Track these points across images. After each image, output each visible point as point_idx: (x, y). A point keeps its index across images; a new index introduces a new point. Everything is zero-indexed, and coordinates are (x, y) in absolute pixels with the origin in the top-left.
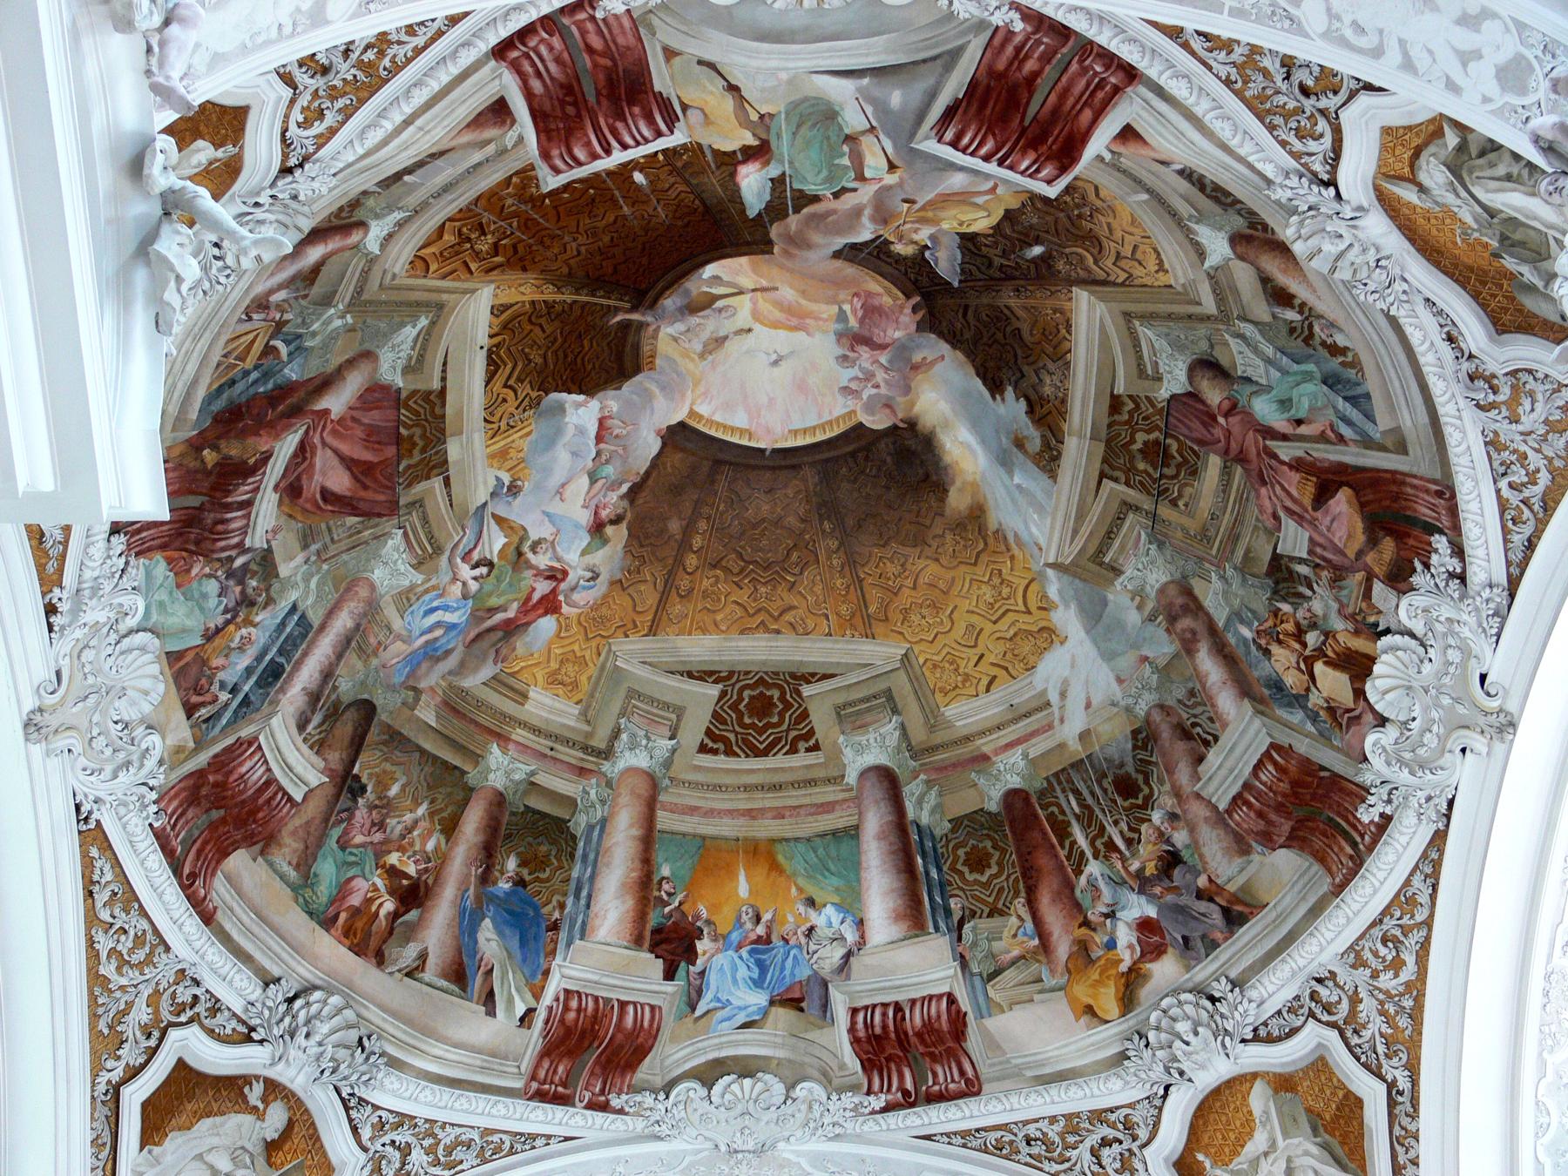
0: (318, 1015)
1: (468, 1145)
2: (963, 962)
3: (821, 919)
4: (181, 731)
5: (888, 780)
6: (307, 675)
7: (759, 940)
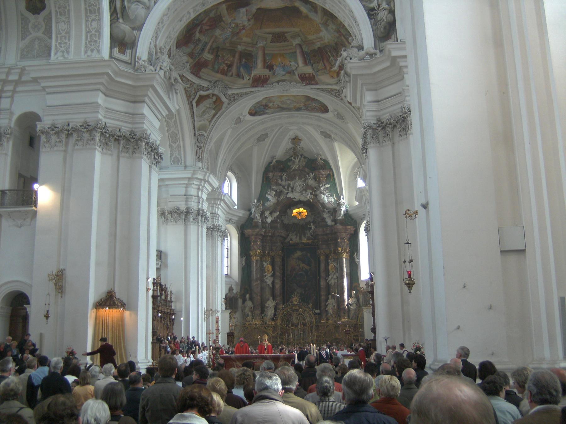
0: (218, 84)
1: (243, 94)
2: (313, 69)
3: (292, 64)
4: (191, 60)
5: (300, 45)
6: (208, 47)
7: (283, 66)
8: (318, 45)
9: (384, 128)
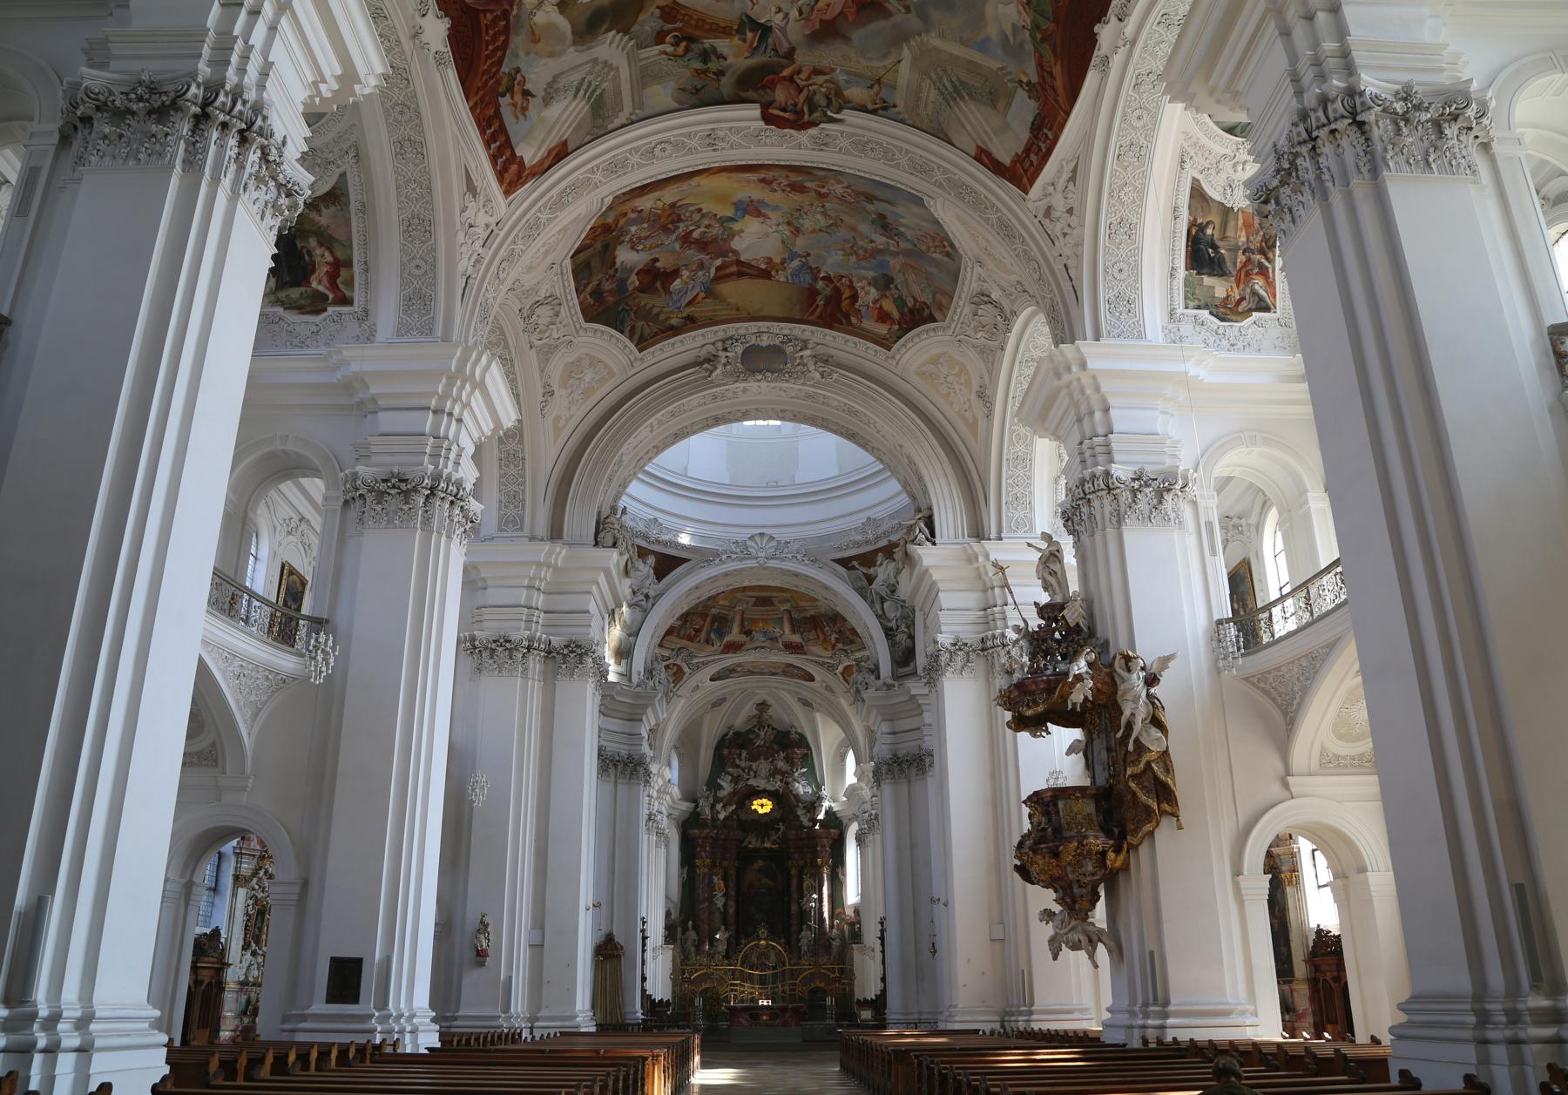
5: (789, 612)
8: (812, 612)
9: (900, 764)
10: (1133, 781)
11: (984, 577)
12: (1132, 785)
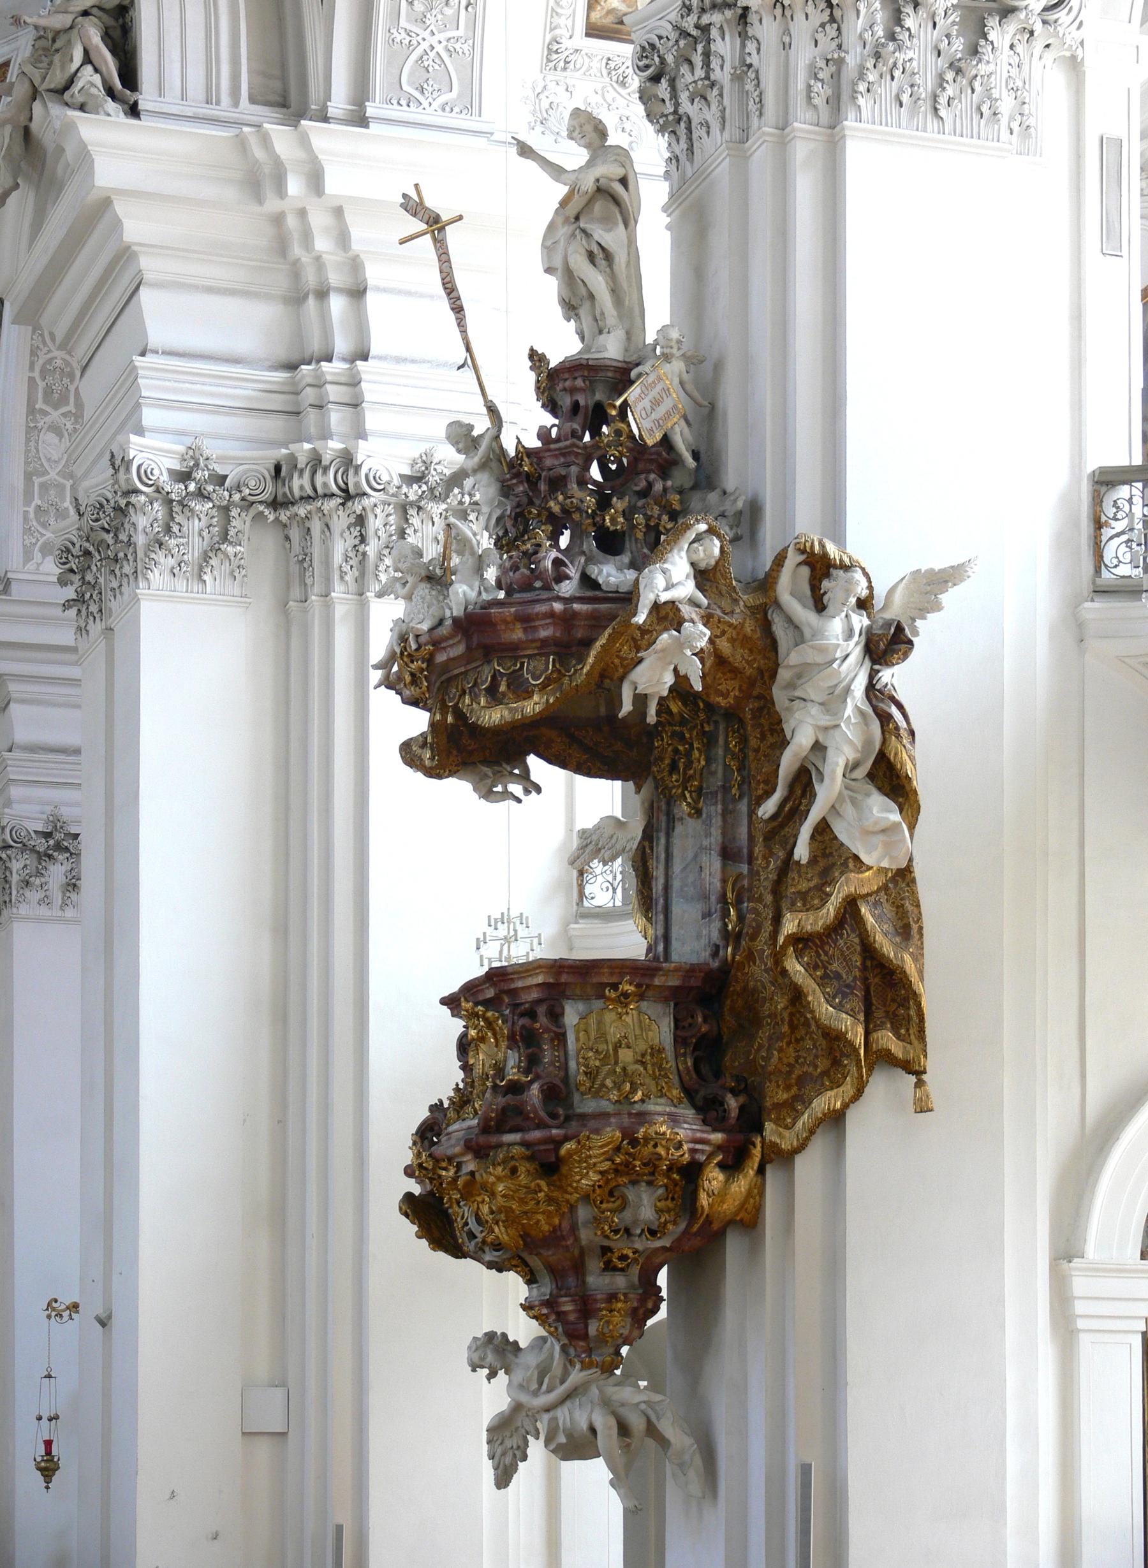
10: (799, 956)
11: (297, 250)
12: (795, 967)
